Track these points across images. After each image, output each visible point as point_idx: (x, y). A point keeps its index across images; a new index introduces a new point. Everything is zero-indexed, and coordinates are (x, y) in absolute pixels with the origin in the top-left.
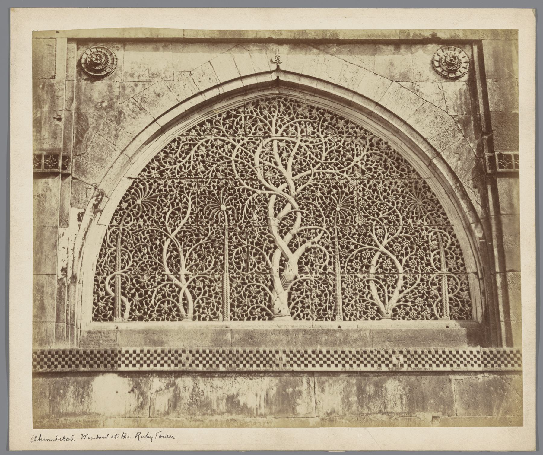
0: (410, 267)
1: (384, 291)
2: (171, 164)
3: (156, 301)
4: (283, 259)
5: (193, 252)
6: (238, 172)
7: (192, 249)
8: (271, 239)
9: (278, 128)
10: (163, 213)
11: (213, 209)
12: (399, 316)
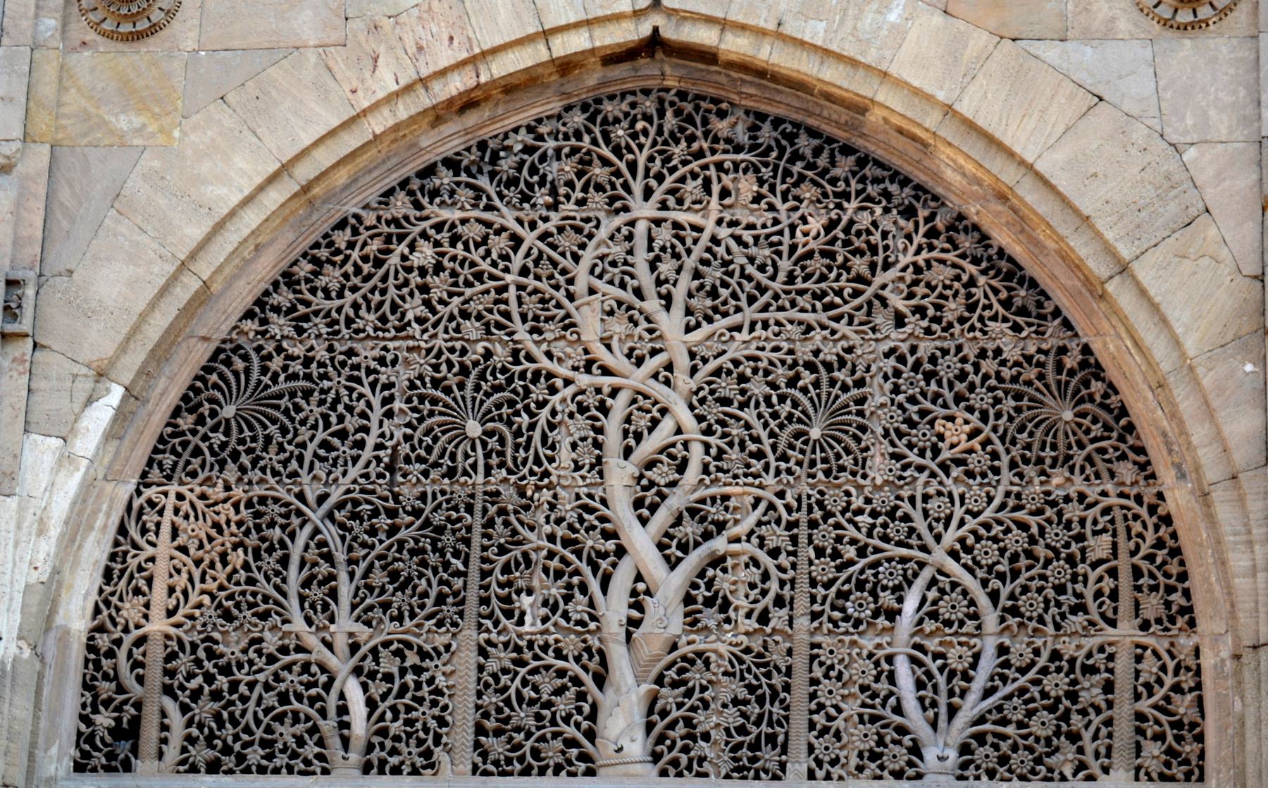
0: (1022, 616)
1: (935, 688)
2: (328, 296)
3: (261, 715)
4: (641, 586)
5: (377, 563)
6: (524, 318)
7: (373, 554)
9: (653, 183)
10: (298, 446)
11: (444, 432)
12: (978, 767)
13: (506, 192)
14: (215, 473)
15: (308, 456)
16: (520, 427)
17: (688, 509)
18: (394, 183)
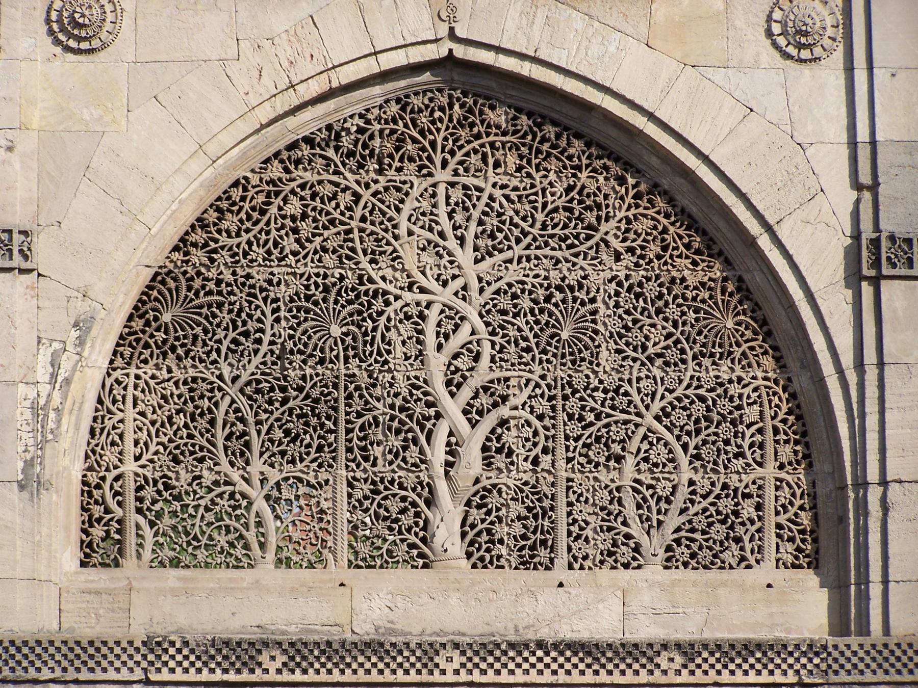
0: (703, 460)
1: (649, 508)
2: (229, 236)
3: (204, 528)
4: (453, 440)
6: (365, 252)
8: (430, 398)
10: (215, 342)
11: (315, 333)
12: (677, 561)
13: (347, 161)
14: (160, 361)
15: (224, 350)
16: (366, 330)
17: (482, 387)
18: (270, 155)
